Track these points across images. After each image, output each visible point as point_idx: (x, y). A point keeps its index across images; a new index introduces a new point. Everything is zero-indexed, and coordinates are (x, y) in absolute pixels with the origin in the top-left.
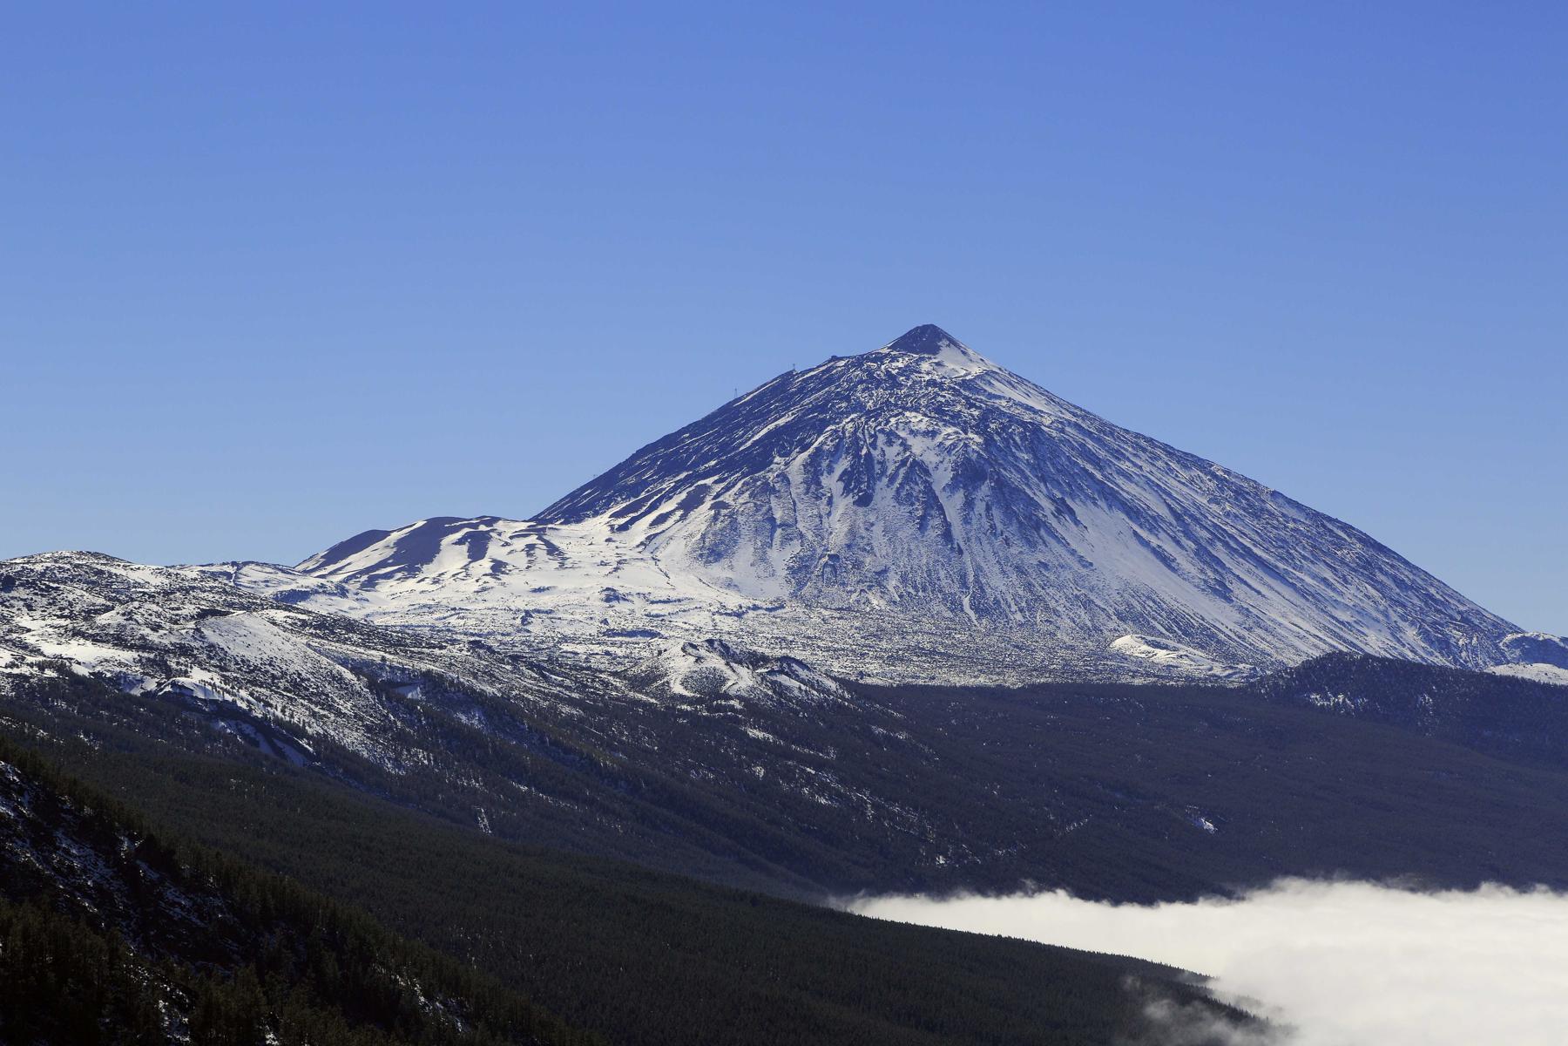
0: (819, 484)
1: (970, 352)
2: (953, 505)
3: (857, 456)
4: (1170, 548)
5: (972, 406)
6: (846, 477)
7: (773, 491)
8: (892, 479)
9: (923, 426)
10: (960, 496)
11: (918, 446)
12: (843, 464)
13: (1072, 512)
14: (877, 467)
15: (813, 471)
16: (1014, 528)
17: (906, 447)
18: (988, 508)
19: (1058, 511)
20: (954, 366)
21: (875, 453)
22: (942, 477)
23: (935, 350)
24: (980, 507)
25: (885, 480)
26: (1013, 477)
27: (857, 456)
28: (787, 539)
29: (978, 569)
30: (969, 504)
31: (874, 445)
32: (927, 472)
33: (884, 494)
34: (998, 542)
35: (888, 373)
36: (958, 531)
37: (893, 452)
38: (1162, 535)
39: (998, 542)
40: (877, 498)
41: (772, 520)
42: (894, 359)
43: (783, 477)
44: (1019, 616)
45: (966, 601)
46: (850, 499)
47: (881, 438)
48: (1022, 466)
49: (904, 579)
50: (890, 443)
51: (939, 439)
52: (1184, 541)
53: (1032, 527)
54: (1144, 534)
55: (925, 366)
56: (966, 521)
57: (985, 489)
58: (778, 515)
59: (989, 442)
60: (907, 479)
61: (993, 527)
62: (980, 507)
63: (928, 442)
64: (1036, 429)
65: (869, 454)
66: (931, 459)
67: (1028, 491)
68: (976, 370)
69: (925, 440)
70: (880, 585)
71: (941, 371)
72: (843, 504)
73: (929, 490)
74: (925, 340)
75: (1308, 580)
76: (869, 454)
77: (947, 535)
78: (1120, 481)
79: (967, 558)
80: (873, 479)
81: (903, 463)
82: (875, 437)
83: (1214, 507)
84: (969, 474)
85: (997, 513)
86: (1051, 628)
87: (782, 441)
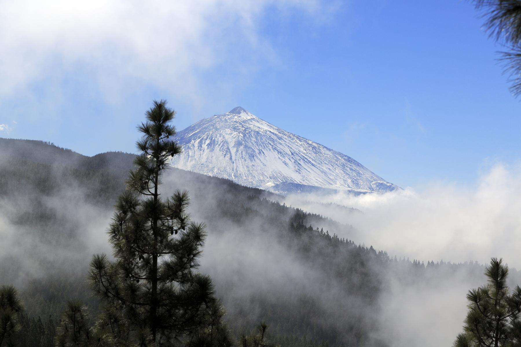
0: (201, 147)
1: (249, 113)
2: (233, 151)
3: (211, 140)
4: (287, 161)
5: (243, 127)
6: (209, 145)
7: (190, 148)
8: (219, 145)
9: (229, 132)
10: (235, 149)
11: (227, 137)
12: (208, 142)
13: (263, 153)
14: (216, 142)
15: (201, 143)
16: (248, 156)
17: (224, 137)
18: (242, 152)
19: (260, 153)
20: (244, 116)
21: (216, 139)
22: (231, 145)
23: (239, 113)
24: (240, 152)
25: (218, 145)
26: (250, 145)
27: (211, 140)
28: (192, 160)
29: (237, 166)
30: (237, 151)
31: (216, 137)
32: (227, 143)
33: (217, 148)
34: (243, 160)
35: (226, 120)
36: (233, 158)
37: (220, 139)
38: (286, 158)
39: (243, 160)
40: (215, 150)
41: (189, 156)
42: (229, 115)
43: (193, 145)
44: (245, 178)
45: (233, 174)
46: (208, 150)
47: (218, 135)
48: (252, 141)
49: (219, 169)
50: (220, 136)
51: (232, 135)
52: (292, 160)
53: (252, 156)
54: (281, 158)
55: (236, 117)
56: (236, 155)
57: (242, 147)
58: (190, 154)
59: (245, 136)
60: (223, 145)
61: (242, 157)
62: (240, 152)
63: (230, 136)
64: (258, 133)
65: (214, 140)
66: (229, 140)
67: (253, 148)
68: (249, 118)
69: (231, 137)
70: (212, 171)
71: (240, 118)
72: (206, 151)
73: (228, 148)
74: (236, 111)
75: (325, 169)
76: (214, 140)
77: (231, 159)
78: (278, 145)
79: (235, 164)
80: (215, 145)
81: (223, 141)
82: (217, 135)
83: (305, 151)
84: (238, 144)
85: (244, 153)
86: (252, 180)
87: (195, 137)
